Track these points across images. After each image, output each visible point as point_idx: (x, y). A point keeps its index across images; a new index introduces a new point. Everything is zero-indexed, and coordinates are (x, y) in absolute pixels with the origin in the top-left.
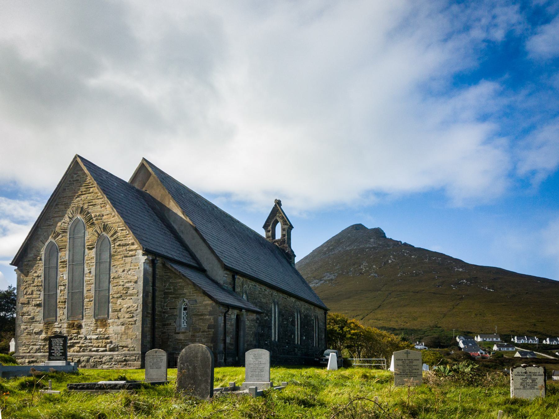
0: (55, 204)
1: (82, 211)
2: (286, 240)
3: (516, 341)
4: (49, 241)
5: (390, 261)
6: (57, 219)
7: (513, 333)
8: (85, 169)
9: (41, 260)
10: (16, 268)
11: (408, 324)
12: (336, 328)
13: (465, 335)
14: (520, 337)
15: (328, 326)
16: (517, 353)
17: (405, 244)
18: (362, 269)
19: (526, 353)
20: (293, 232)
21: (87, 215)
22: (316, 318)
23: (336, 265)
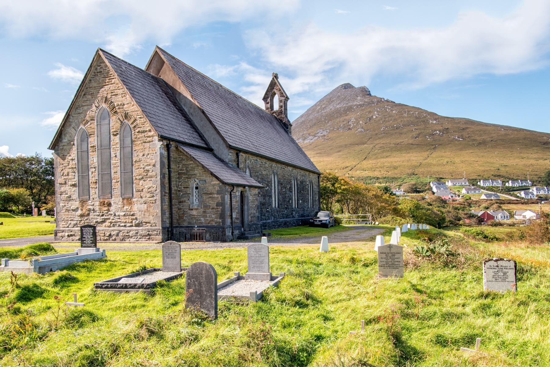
0: (83, 93)
1: (106, 100)
2: (283, 110)
3: (482, 185)
4: (80, 128)
5: (374, 117)
6: (86, 108)
7: (479, 178)
8: (106, 61)
9: (74, 144)
10: (53, 151)
11: (390, 173)
12: (328, 185)
13: (438, 180)
14: (485, 180)
15: (321, 183)
16: (483, 195)
17: (387, 101)
18: (350, 125)
19: (490, 195)
20: (289, 103)
21: (110, 104)
22: (311, 182)
23: (328, 122)
